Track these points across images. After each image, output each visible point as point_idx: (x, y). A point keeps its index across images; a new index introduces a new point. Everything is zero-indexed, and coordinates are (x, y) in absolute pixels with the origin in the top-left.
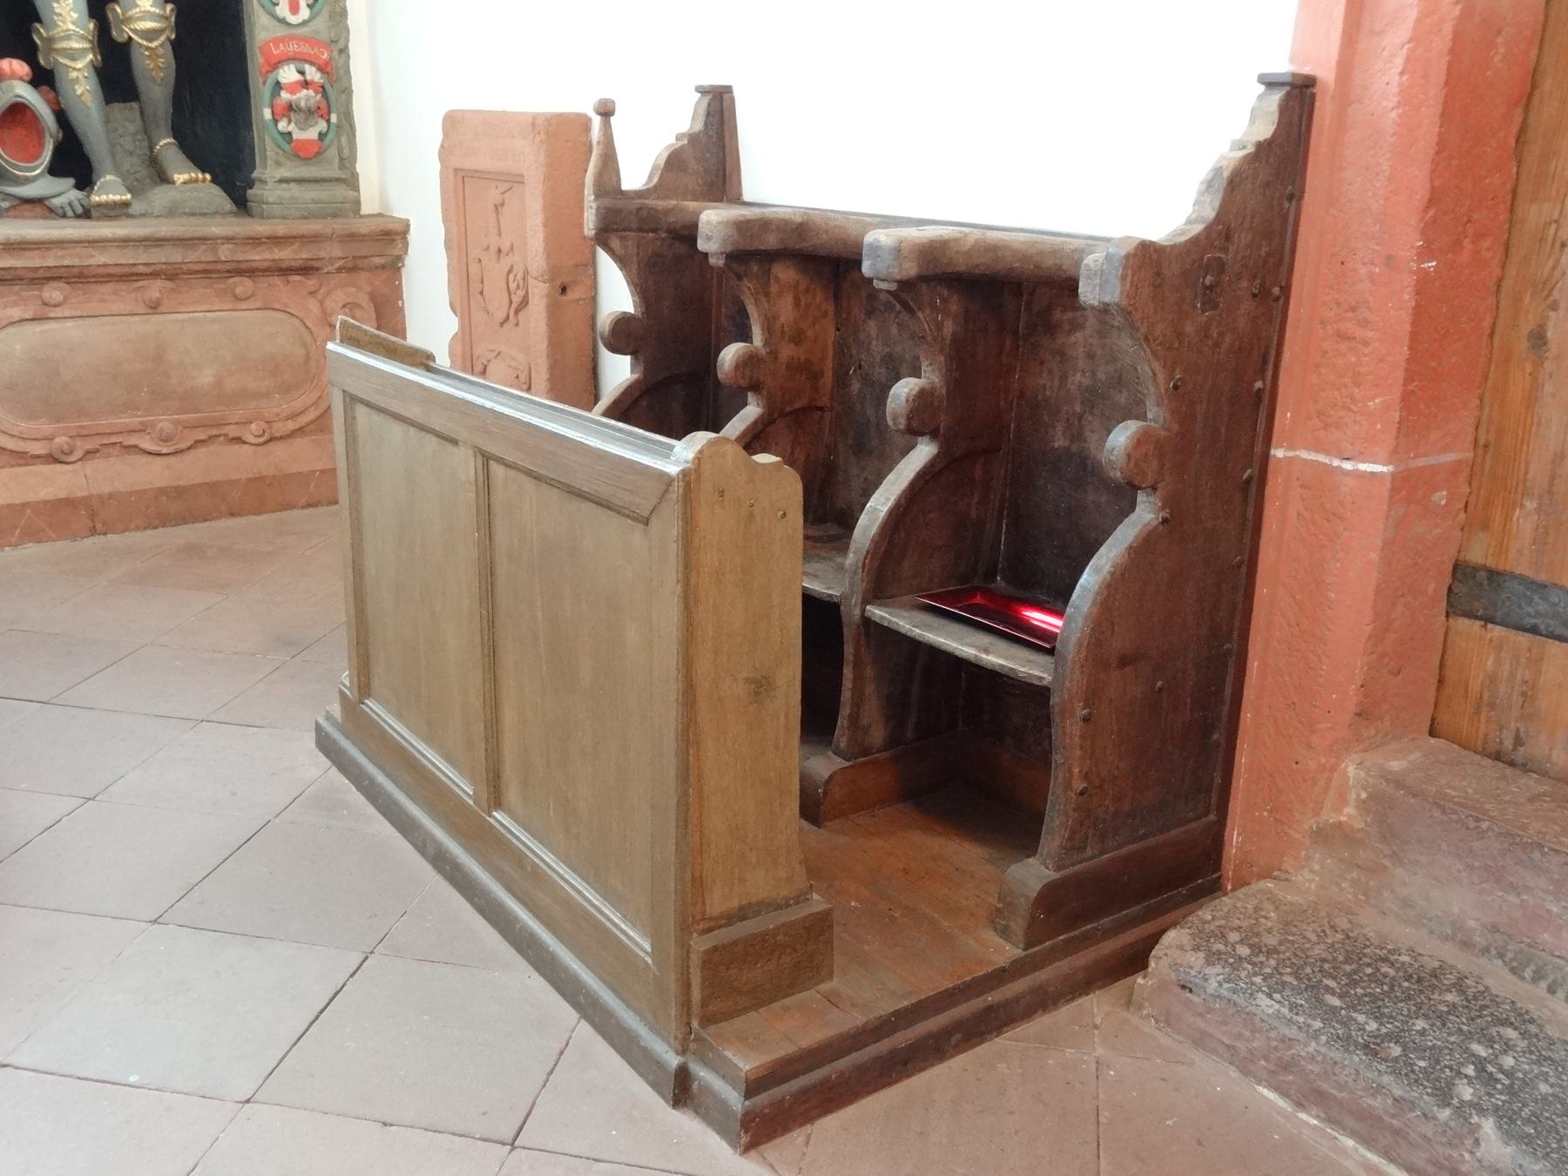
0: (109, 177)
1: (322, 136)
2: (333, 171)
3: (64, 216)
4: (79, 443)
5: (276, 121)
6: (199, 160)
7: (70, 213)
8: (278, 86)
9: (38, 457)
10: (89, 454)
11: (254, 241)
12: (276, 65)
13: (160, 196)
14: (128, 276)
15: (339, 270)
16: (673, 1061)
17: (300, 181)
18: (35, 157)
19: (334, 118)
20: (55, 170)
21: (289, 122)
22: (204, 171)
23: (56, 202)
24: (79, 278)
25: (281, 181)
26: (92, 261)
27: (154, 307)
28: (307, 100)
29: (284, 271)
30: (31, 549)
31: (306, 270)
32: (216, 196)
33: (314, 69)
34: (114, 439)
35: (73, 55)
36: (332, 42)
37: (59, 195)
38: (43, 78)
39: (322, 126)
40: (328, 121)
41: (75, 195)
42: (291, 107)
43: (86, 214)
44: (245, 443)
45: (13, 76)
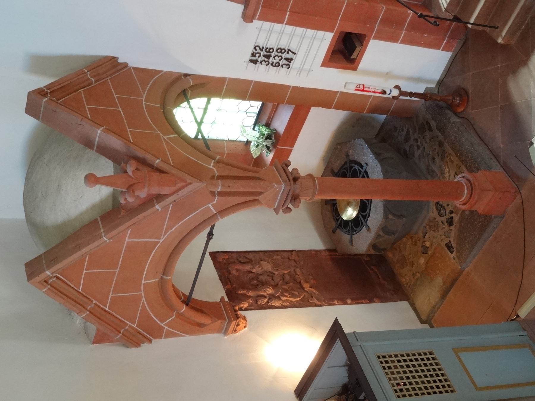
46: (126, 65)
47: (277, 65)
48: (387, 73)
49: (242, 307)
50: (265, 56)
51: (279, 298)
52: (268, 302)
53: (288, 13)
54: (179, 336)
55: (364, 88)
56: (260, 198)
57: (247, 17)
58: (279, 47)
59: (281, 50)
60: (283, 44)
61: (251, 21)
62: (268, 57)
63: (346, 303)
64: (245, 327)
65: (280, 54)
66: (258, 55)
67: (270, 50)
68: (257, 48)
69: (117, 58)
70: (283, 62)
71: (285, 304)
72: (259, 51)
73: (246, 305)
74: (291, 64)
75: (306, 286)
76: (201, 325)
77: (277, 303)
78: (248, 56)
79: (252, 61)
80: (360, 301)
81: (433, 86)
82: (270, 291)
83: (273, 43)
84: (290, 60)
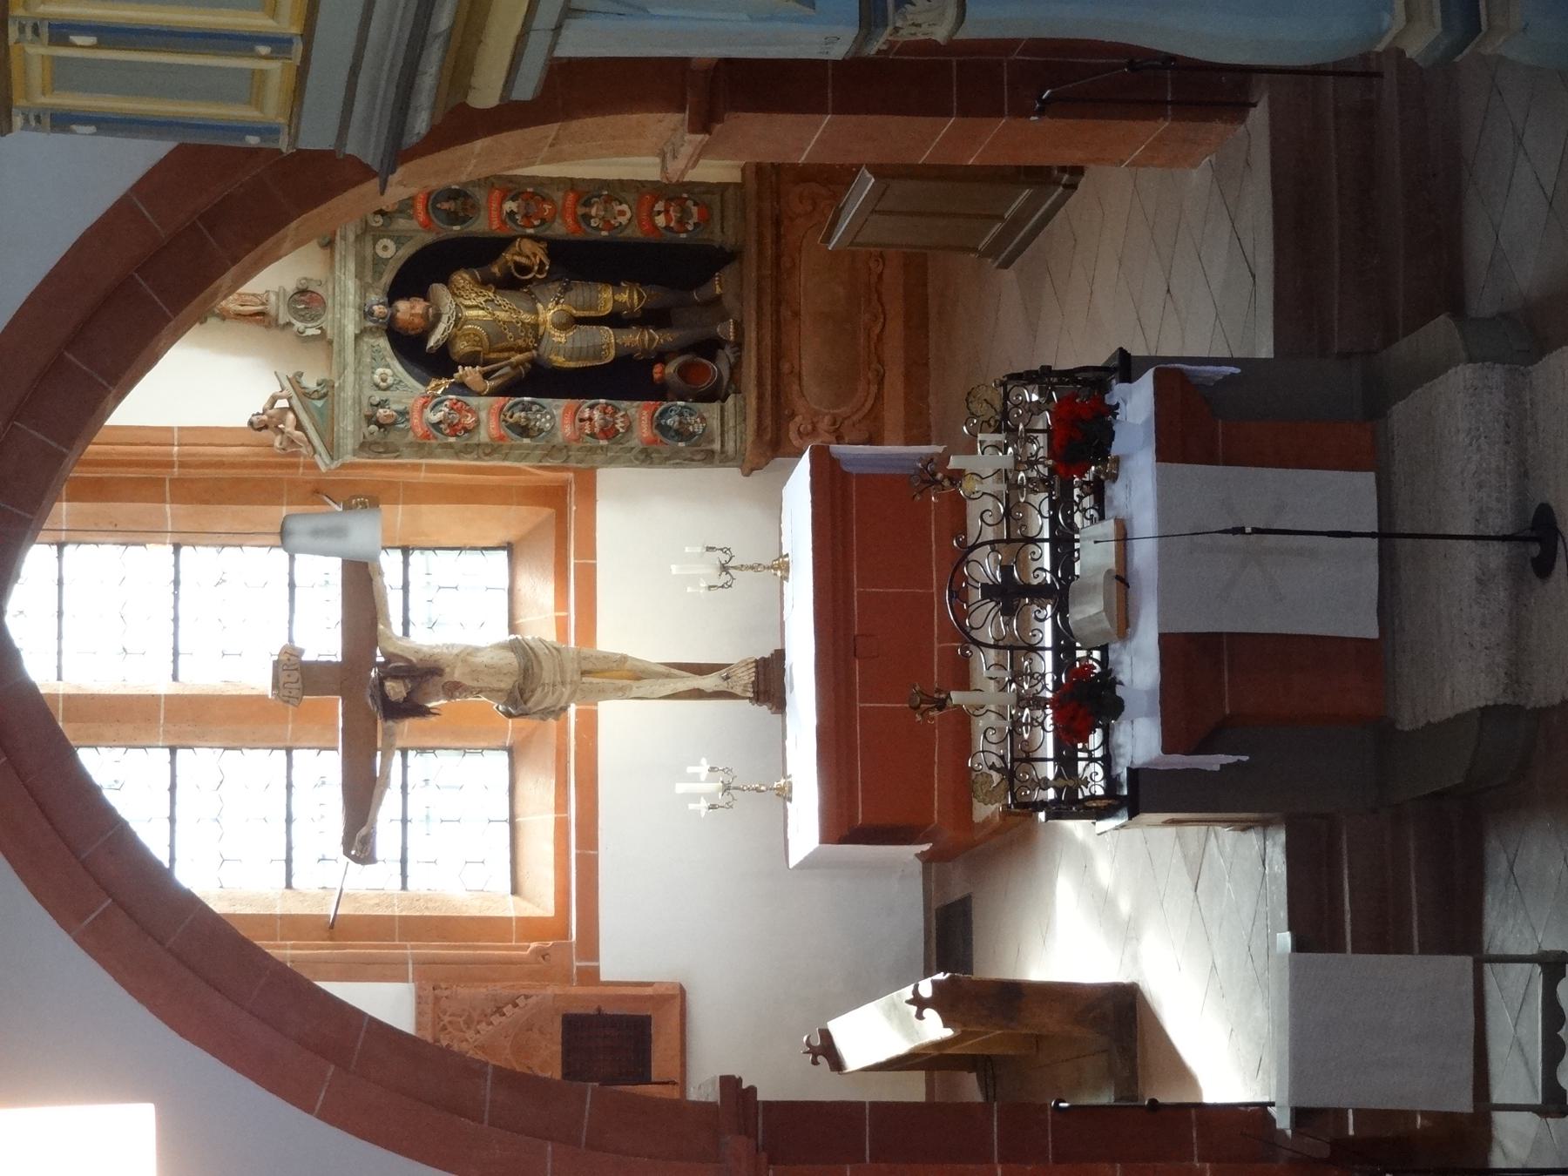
0: (718, 330)
1: (696, 204)
2: (717, 198)
3: (740, 357)
4: (873, 366)
5: (687, 231)
6: (706, 279)
7: (739, 354)
8: (667, 228)
9: (879, 389)
10: (880, 361)
11: (760, 253)
12: (655, 227)
13: (729, 302)
14: (778, 325)
15: (778, 203)
16: (1060, 189)
17: (723, 218)
18: (706, 368)
19: (685, 196)
20: (713, 359)
21: (687, 223)
22: (713, 276)
23: (732, 360)
24: (778, 356)
25: (723, 232)
26: (769, 343)
27: (796, 314)
28: (676, 212)
29: (778, 239)
30: (932, 399)
31: (777, 223)
32: (729, 272)
33: (657, 205)
34: (873, 347)
35: (652, 340)
36: (638, 191)
37: (728, 357)
38: (662, 356)
39: (690, 203)
40: (686, 199)
41: (728, 350)
42: (681, 222)
43: (739, 345)
44: (882, 272)
45: (662, 372)
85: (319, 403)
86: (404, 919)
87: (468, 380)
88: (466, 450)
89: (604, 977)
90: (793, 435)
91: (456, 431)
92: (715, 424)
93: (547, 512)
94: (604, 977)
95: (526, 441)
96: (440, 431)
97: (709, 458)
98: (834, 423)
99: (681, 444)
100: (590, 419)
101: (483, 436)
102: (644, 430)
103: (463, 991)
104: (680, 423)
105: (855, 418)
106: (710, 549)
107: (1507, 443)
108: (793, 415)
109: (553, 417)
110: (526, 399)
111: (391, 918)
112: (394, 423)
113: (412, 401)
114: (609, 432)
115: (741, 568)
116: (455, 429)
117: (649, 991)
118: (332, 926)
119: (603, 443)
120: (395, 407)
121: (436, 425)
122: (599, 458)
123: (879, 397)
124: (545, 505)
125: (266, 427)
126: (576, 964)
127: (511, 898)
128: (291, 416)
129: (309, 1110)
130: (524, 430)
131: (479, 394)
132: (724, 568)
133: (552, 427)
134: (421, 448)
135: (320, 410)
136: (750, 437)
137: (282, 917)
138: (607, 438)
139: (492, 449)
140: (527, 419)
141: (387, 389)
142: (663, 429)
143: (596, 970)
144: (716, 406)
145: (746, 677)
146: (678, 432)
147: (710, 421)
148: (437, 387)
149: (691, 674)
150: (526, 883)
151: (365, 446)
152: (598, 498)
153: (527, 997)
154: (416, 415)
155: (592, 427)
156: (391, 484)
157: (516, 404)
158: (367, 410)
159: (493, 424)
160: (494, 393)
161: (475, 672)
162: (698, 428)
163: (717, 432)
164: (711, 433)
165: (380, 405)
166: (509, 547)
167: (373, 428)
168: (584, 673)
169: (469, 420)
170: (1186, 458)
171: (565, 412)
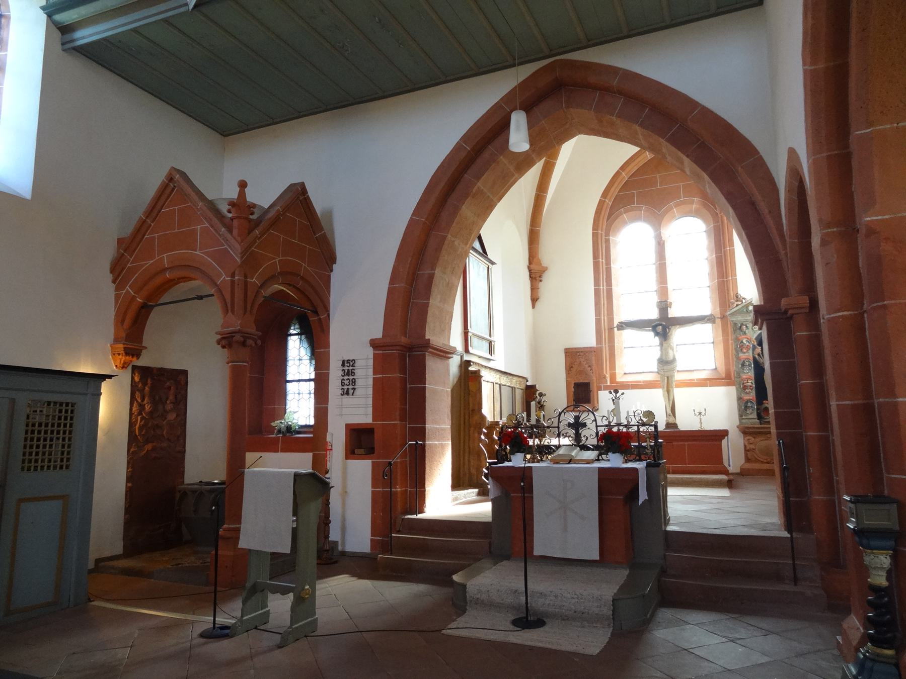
46: (332, 271)
47: (343, 384)
48: (346, 492)
49: (135, 374)
50: (348, 370)
51: (140, 414)
52: (137, 401)
53: (381, 376)
54: (115, 308)
55: (329, 450)
56: (230, 313)
57: (374, 344)
58: (356, 380)
59: (354, 382)
60: (359, 383)
61: (371, 346)
62: (348, 374)
63: (128, 480)
64: (116, 366)
65: (351, 383)
66: (348, 365)
67: (353, 374)
68: (354, 362)
69: (335, 263)
70: (346, 387)
71: (134, 417)
72: (351, 364)
73: (137, 379)
74: (346, 396)
75: (149, 447)
76: (123, 321)
77: (136, 409)
78: (346, 358)
79: (343, 361)
80: (128, 497)
81: (340, 548)
82: (147, 408)
83: (359, 373)
84: (347, 393)
85: (745, 310)
86: (614, 346)
87: (757, 349)
88: (737, 352)
89: (599, 392)
90: (748, 437)
91: (740, 347)
92: (750, 417)
93: (724, 376)
94: (599, 392)
95: (740, 366)
96: (741, 343)
97: (741, 416)
98: (753, 449)
99: (743, 407)
100: (748, 382)
101: (741, 355)
102: (746, 397)
103: (594, 358)
104: (749, 407)
105: (755, 455)
106: (705, 410)
107: (575, 612)
108: (754, 438)
109: (748, 373)
110: (753, 365)
111: (614, 343)
112: (742, 331)
113: (749, 335)
114: (745, 388)
115: (701, 419)
116: (742, 347)
117: (596, 402)
118: (611, 329)
119: (742, 386)
120: (747, 331)
121: (742, 342)
122: (738, 386)
123: (763, 462)
124: (726, 374)
125: (737, 298)
126: (602, 385)
127: (623, 372)
128: (740, 303)
129: (413, 215)
130: (743, 365)
131: (753, 353)
132: (700, 413)
133: (745, 373)
134: (737, 339)
135: (743, 311)
136: (746, 426)
137: (613, 317)
138: (743, 387)
139: (738, 358)
140: (746, 365)
141: (752, 329)
142: (747, 402)
143: (601, 390)
144: (756, 417)
145: (671, 420)
146: (746, 406)
147: (751, 415)
148: (753, 342)
149: (671, 405)
150: (626, 376)
151: (735, 324)
152: (727, 387)
153: (593, 373)
154: (745, 336)
155: (745, 383)
156: (728, 335)
157: (750, 362)
158: (744, 323)
159: (744, 357)
160: (754, 358)
161: (666, 350)
162: (748, 412)
163: (748, 417)
164: (747, 416)
165: (746, 326)
166: (716, 369)
167: (740, 325)
168: (668, 377)
169: (744, 350)
170: (600, 480)
171: (750, 376)
